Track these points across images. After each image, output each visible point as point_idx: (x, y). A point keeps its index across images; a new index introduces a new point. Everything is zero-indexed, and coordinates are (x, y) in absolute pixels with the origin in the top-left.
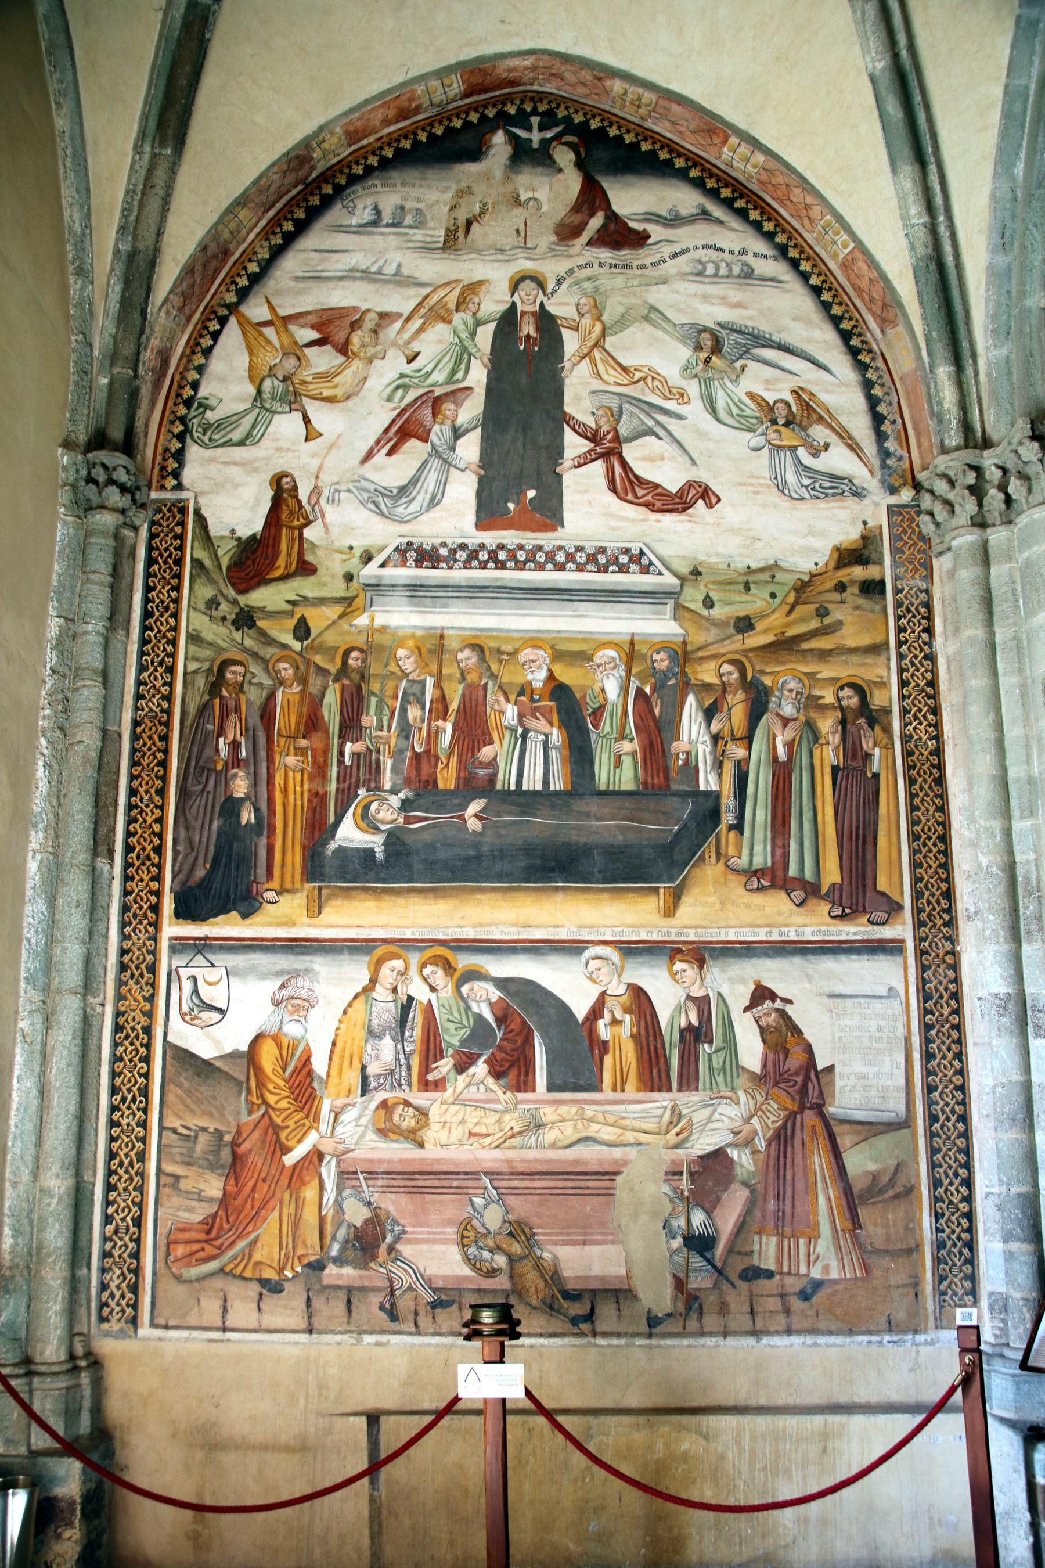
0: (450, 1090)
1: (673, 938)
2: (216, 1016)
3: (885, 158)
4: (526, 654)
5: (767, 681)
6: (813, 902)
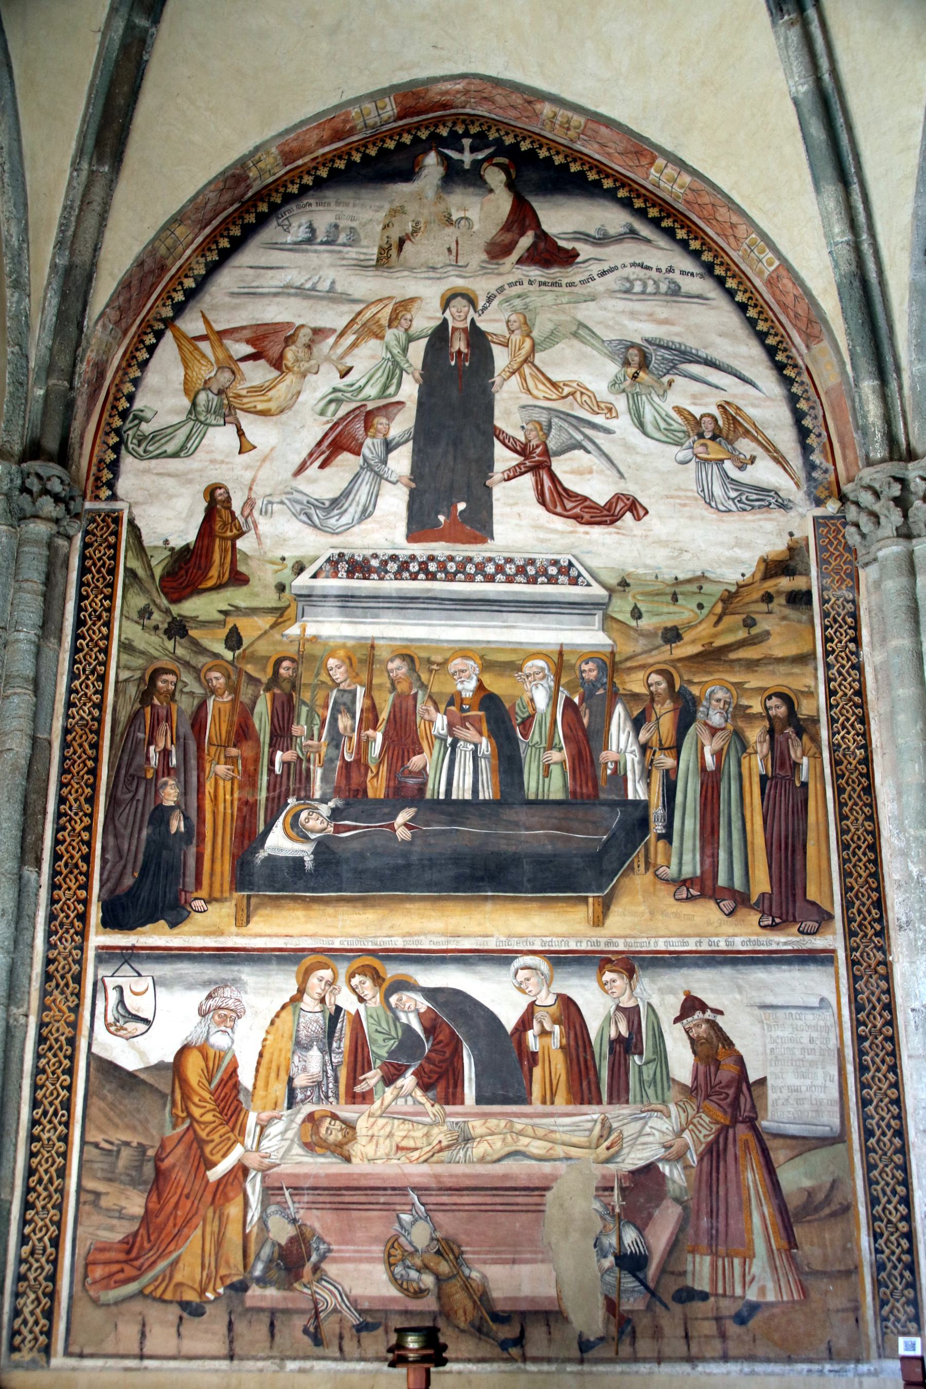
0: (377, 1103)
2: (142, 1027)
3: (809, 178)
4: (456, 664)
5: (695, 691)
6: (742, 912)
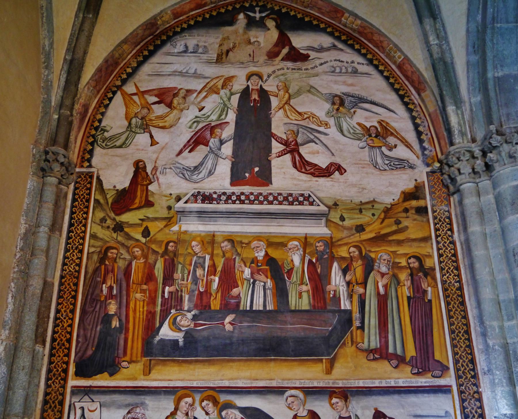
1: (331, 385)
4: (255, 244)
5: (373, 255)
6: (402, 366)
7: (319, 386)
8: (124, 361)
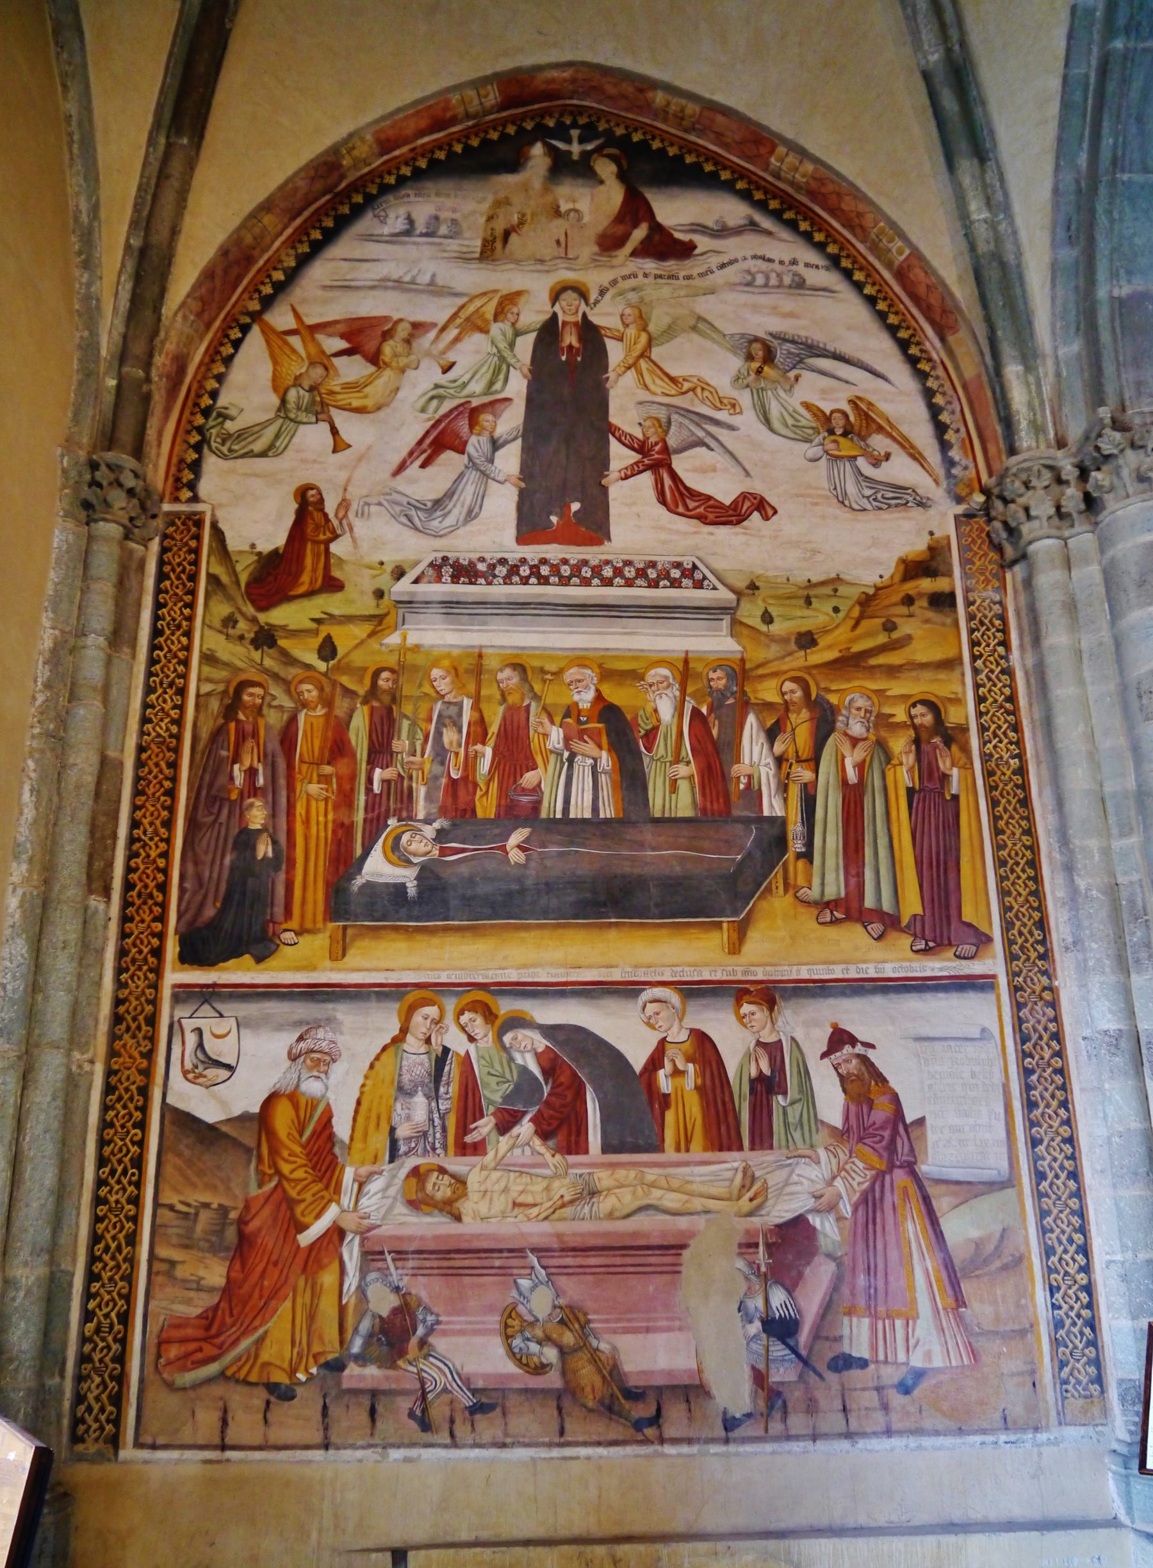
0: (491, 1155)
1: (739, 977)
2: (223, 1073)
4: (572, 673)
5: (833, 699)
6: (893, 935)
7: (714, 978)
8: (286, 930)
